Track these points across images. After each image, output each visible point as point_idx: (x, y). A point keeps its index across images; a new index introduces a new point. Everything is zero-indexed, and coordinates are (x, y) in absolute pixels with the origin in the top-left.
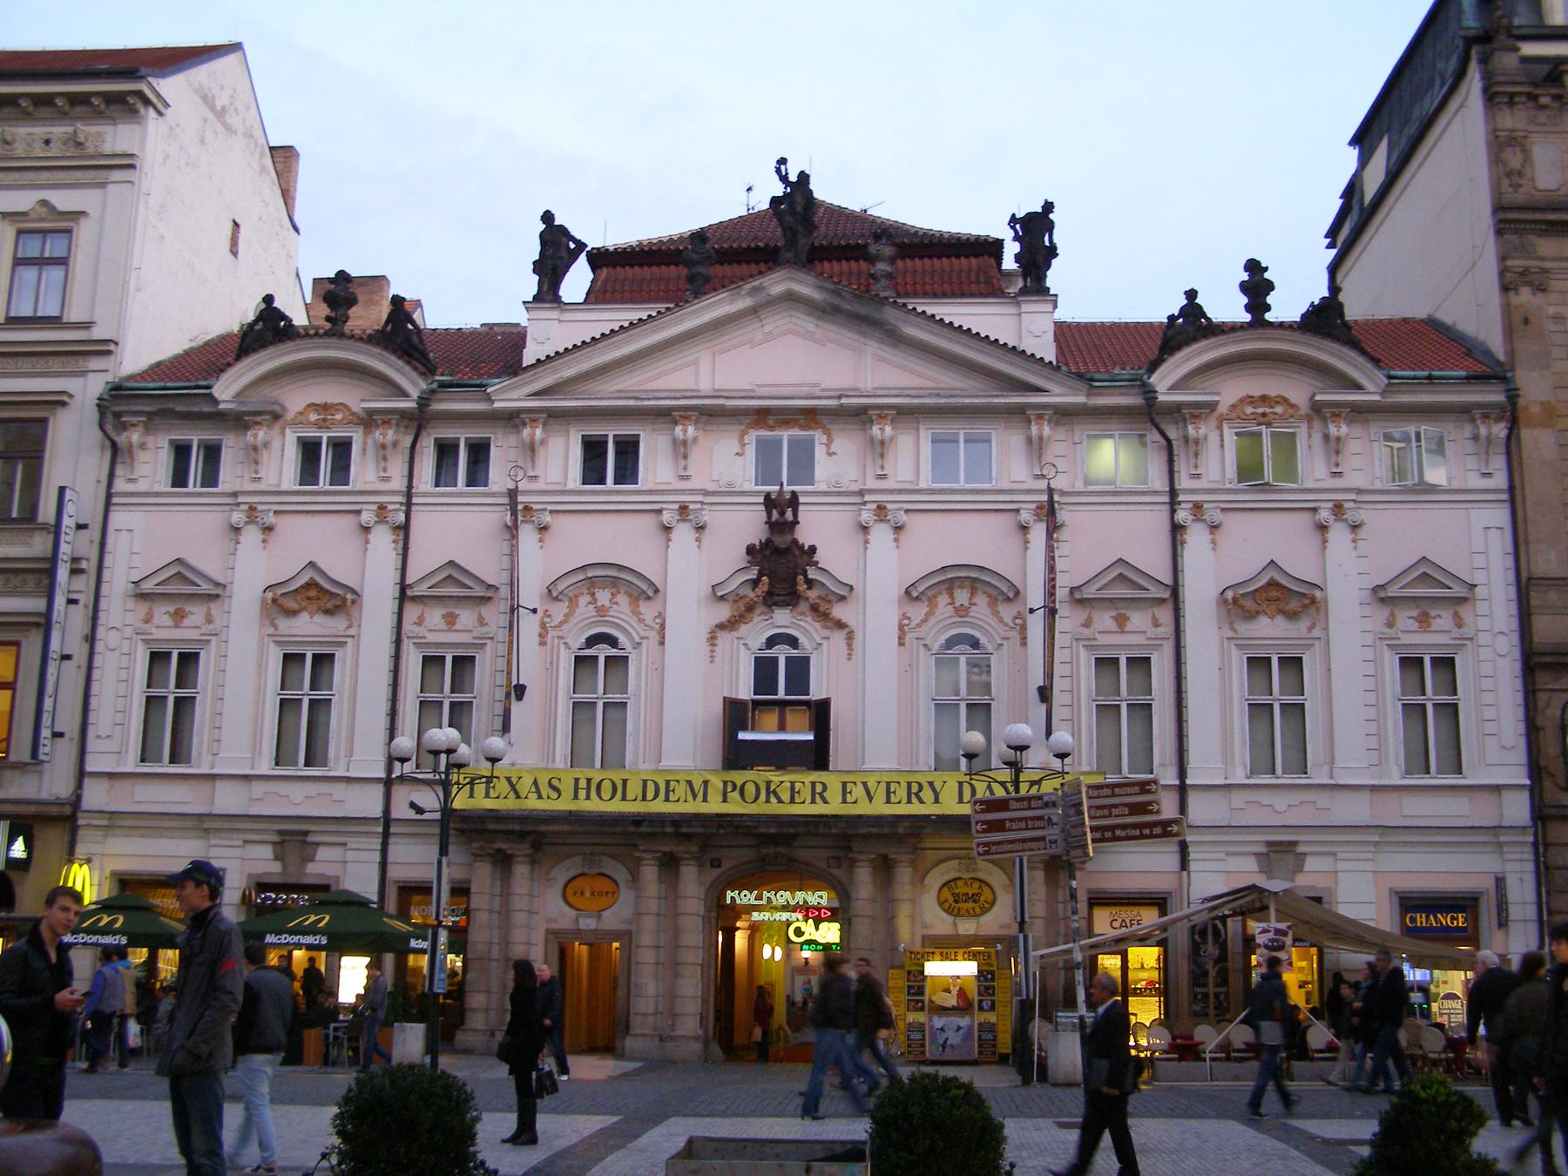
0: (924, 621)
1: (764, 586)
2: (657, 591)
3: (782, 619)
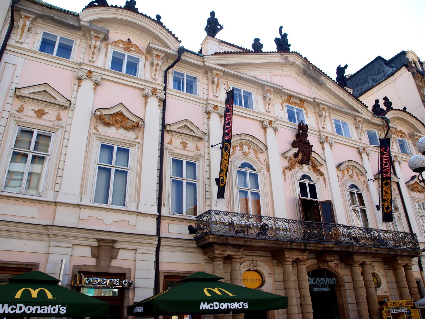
1: (300, 156)
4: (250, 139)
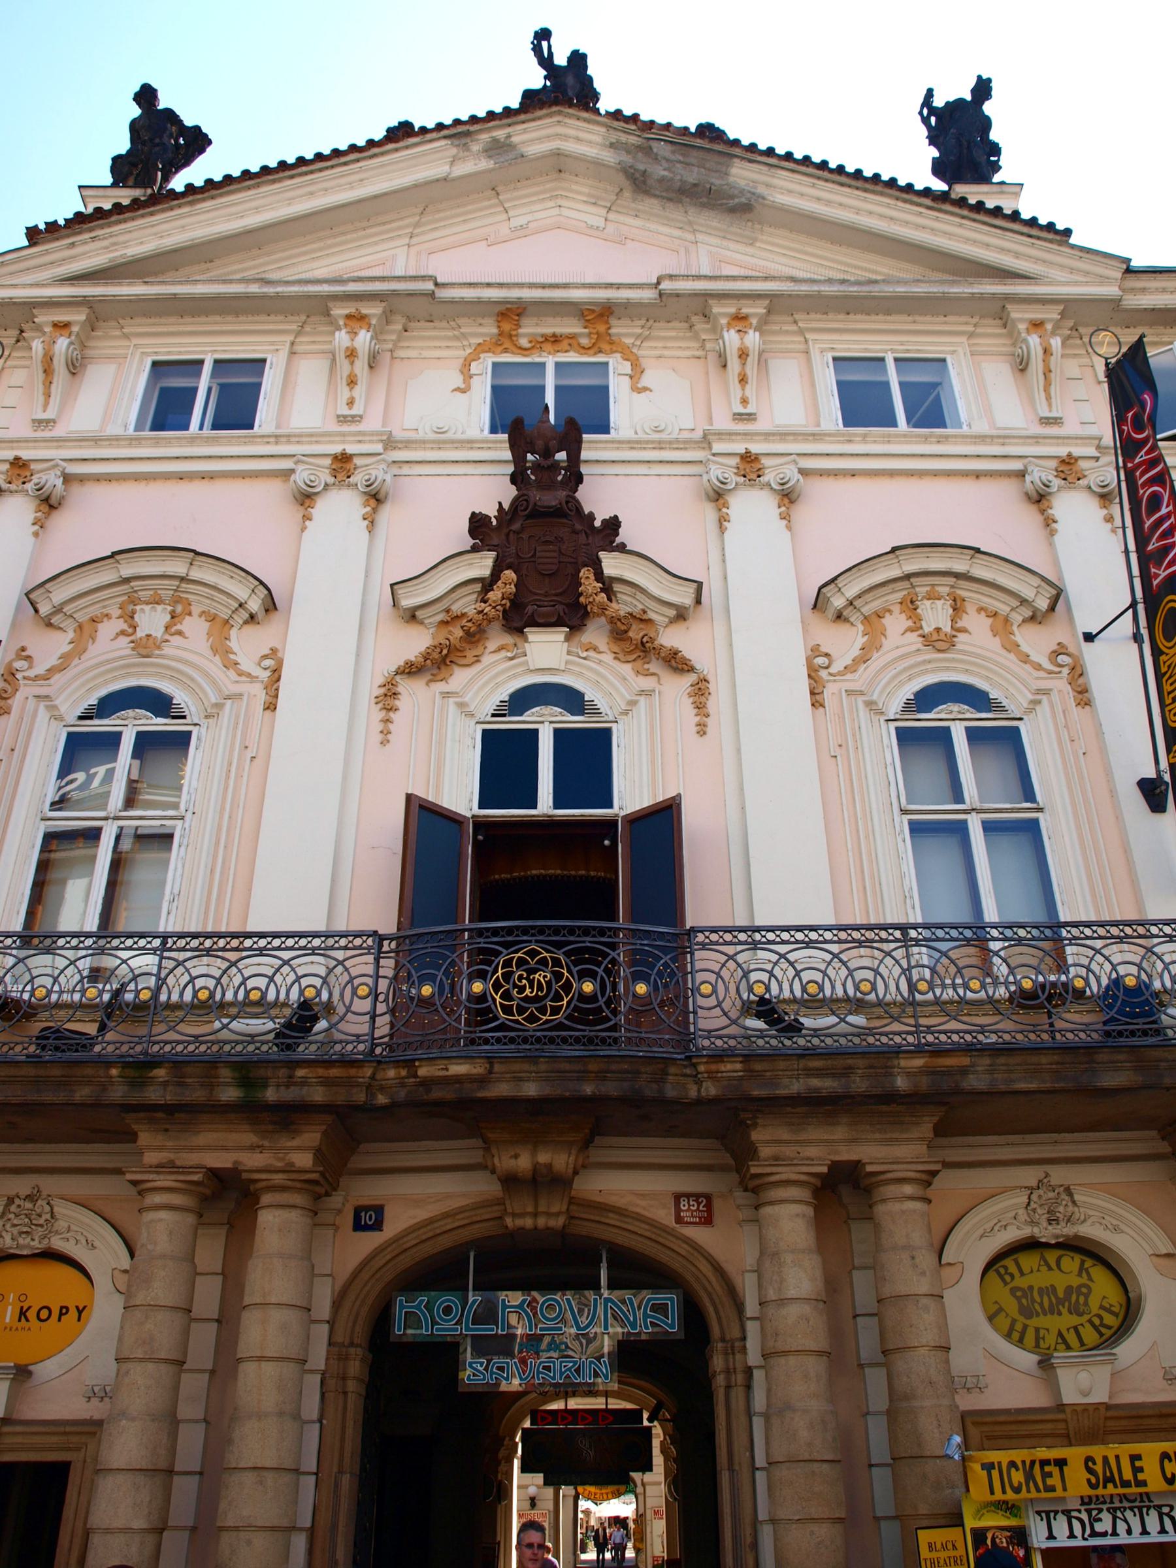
0: (863, 658)
2: (271, 605)
3: (546, 653)
4: (177, 567)
